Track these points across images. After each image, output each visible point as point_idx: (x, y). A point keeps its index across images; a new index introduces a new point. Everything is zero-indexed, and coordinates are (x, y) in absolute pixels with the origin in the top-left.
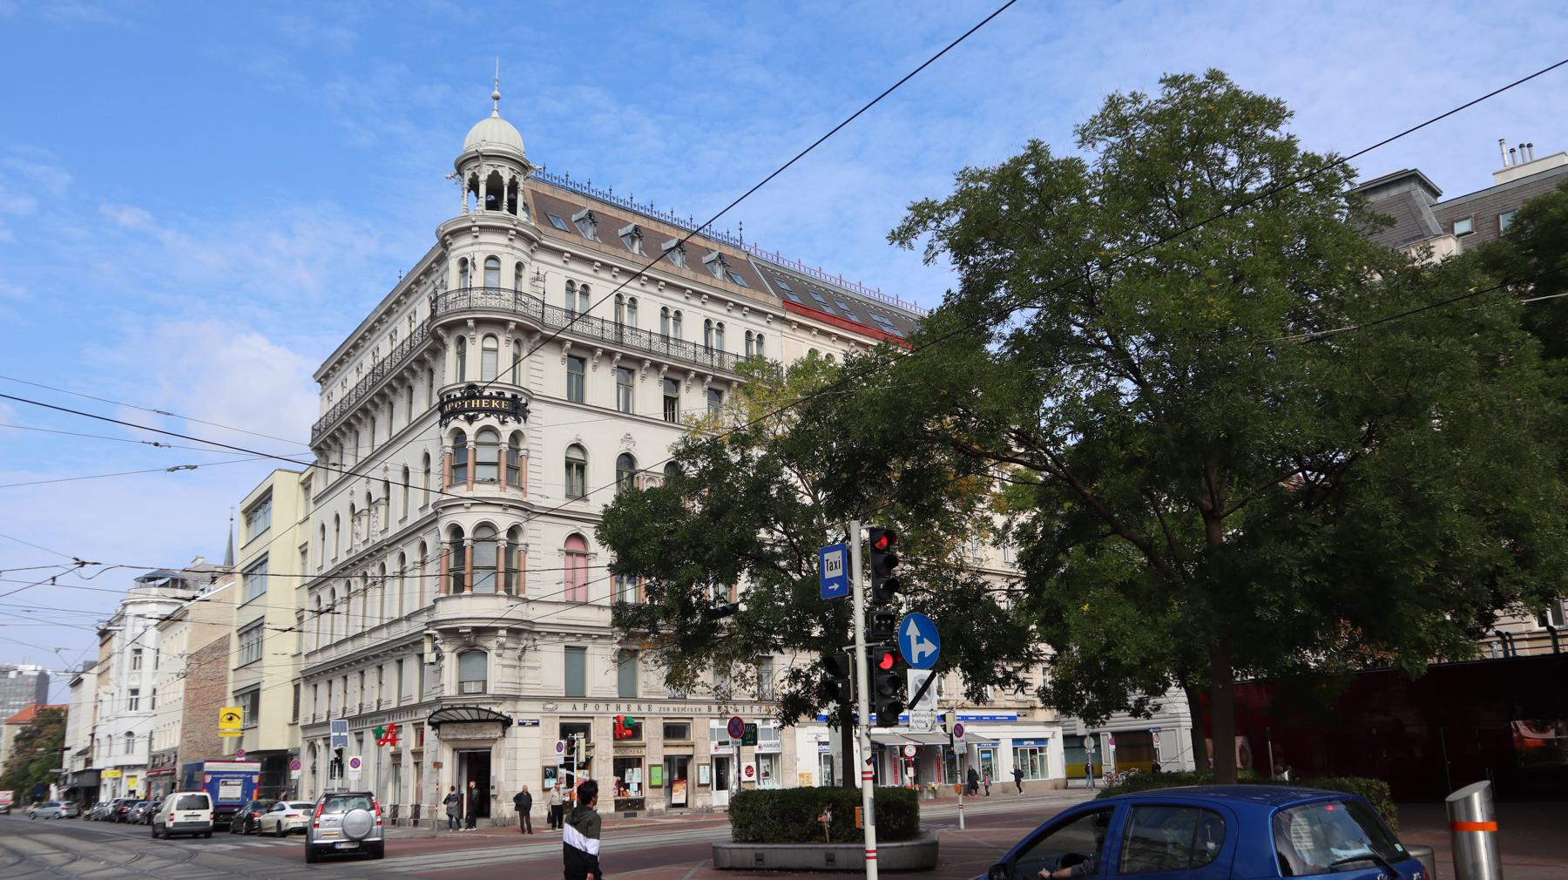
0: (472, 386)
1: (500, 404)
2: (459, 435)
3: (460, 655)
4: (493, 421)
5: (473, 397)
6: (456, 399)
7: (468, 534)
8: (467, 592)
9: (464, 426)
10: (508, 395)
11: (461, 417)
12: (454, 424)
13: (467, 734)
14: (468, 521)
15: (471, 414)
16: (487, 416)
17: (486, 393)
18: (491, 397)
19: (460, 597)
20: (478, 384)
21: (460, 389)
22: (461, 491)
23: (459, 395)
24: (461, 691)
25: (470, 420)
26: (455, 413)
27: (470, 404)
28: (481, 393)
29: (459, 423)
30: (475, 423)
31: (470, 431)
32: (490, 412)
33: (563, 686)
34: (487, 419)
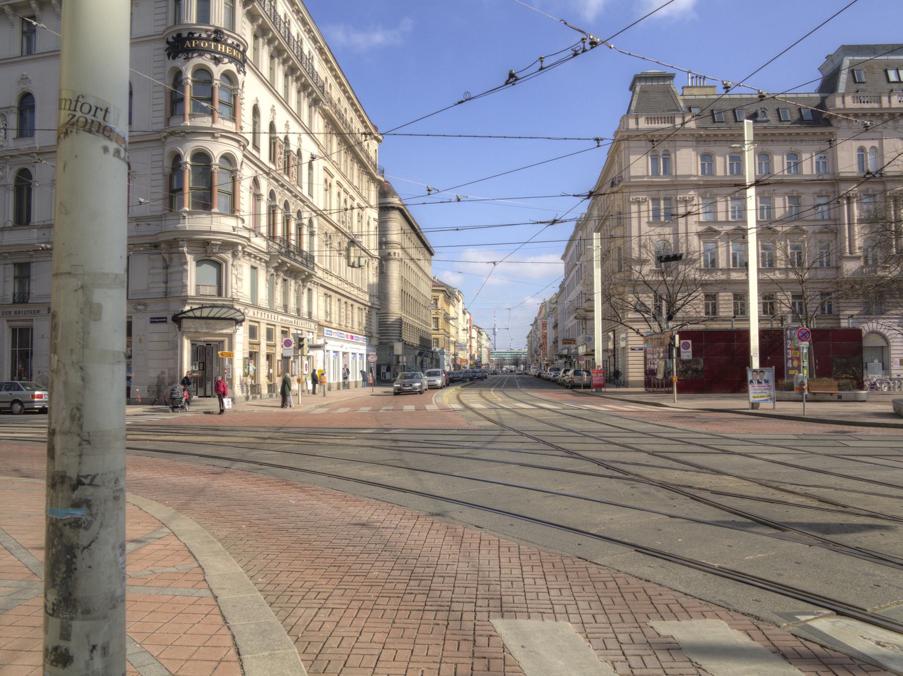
0: (218, 31)
1: (238, 54)
2: (203, 73)
3: (197, 262)
4: (233, 67)
5: (216, 40)
6: (200, 38)
7: (216, 160)
8: (215, 210)
9: (211, 65)
10: (241, 49)
11: (208, 56)
12: (197, 60)
13: (207, 328)
14: (217, 149)
15: (217, 56)
16: (230, 62)
17: (230, 41)
18: (231, 46)
19: (211, 214)
20: (226, 32)
21: (207, 31)
22: (204, 122)
23: (204, 35)
24: (197, 291)
25: (217, 61)
26: (201, 52)
27: (216, 47)
28: (226, 40)
29: (206, 61)
30: (221, 65)
31: (217, 71)
32: (232, 59)
33: (250, 297)
34: (229, 64)
